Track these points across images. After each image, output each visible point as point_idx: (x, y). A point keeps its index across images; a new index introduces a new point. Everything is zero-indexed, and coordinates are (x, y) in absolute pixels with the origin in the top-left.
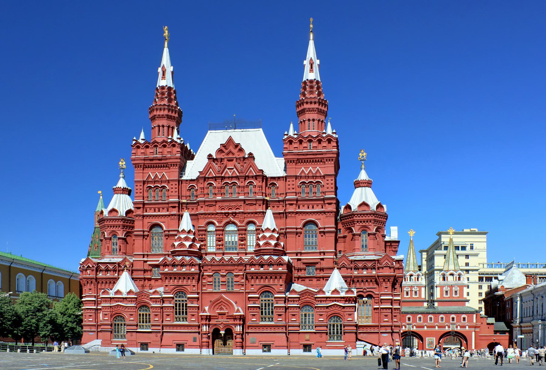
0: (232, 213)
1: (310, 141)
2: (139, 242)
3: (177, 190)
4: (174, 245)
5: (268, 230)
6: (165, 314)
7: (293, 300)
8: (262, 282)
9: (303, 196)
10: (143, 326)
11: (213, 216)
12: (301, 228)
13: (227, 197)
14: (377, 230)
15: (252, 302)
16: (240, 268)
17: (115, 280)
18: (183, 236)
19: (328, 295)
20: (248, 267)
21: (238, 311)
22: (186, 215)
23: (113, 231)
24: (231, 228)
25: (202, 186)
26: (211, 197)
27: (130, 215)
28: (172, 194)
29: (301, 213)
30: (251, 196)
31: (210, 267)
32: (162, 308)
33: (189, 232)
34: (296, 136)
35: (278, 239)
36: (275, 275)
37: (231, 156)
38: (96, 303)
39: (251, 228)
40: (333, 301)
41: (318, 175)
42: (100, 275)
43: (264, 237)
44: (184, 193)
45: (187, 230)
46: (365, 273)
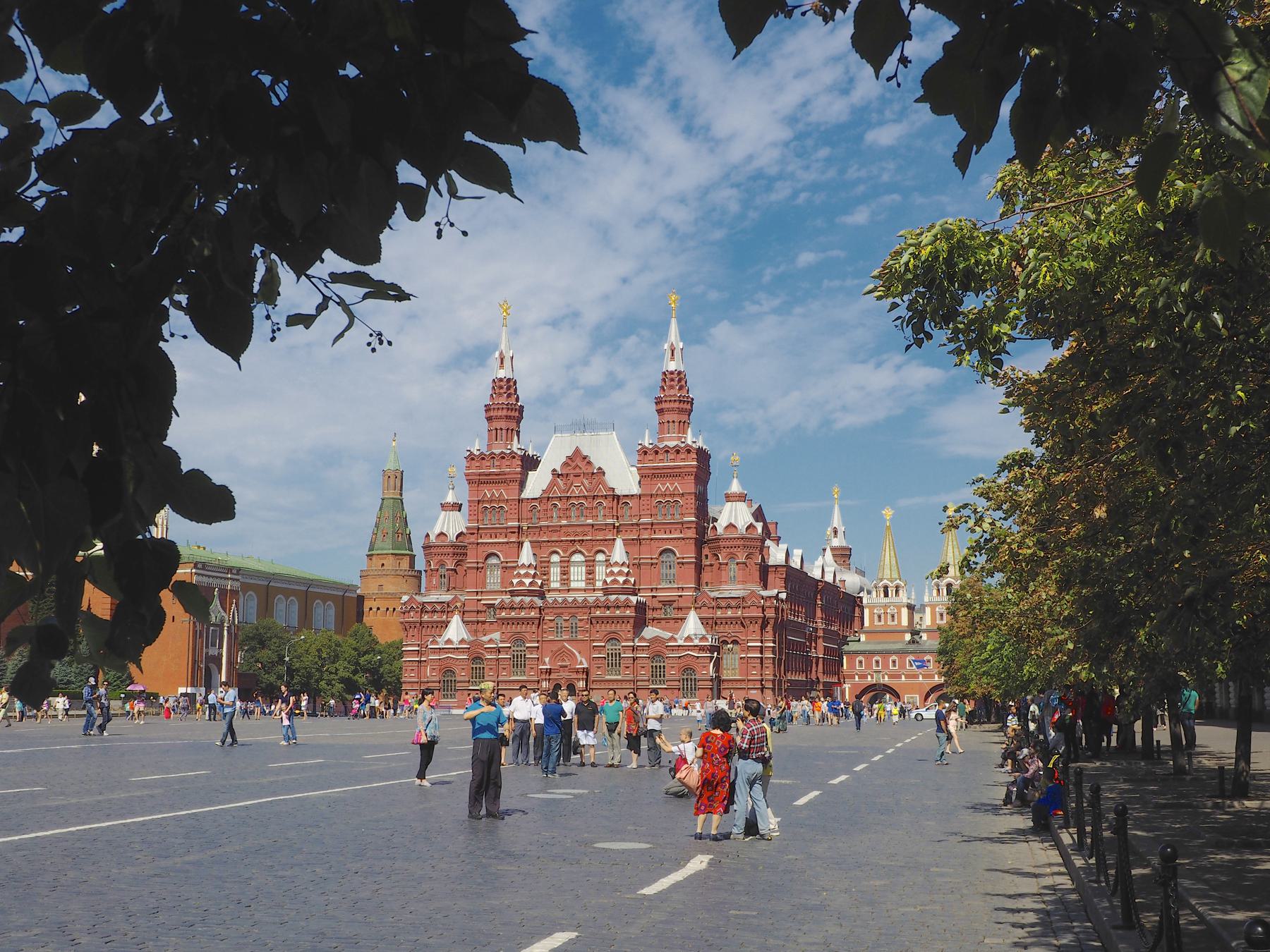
1: (667, 452)
2: (472, 575)
5: (616, 564)
8: (609, 628)
9: (660, 519)
13: (574, 521)
14: (747, 557)
18: (522, 572)
19: (680, 642)
21: (581, 663)
22: (527, 548)
24: (577, 558)
26: (555, 522)
27: (461, 538)
30: (601, 521)
35: (628, 574)
36: (623, 619)
37: (577, 471)
39: (600, 557)
42: (426, 618)
45: (527, 564)
46: (729, 613)
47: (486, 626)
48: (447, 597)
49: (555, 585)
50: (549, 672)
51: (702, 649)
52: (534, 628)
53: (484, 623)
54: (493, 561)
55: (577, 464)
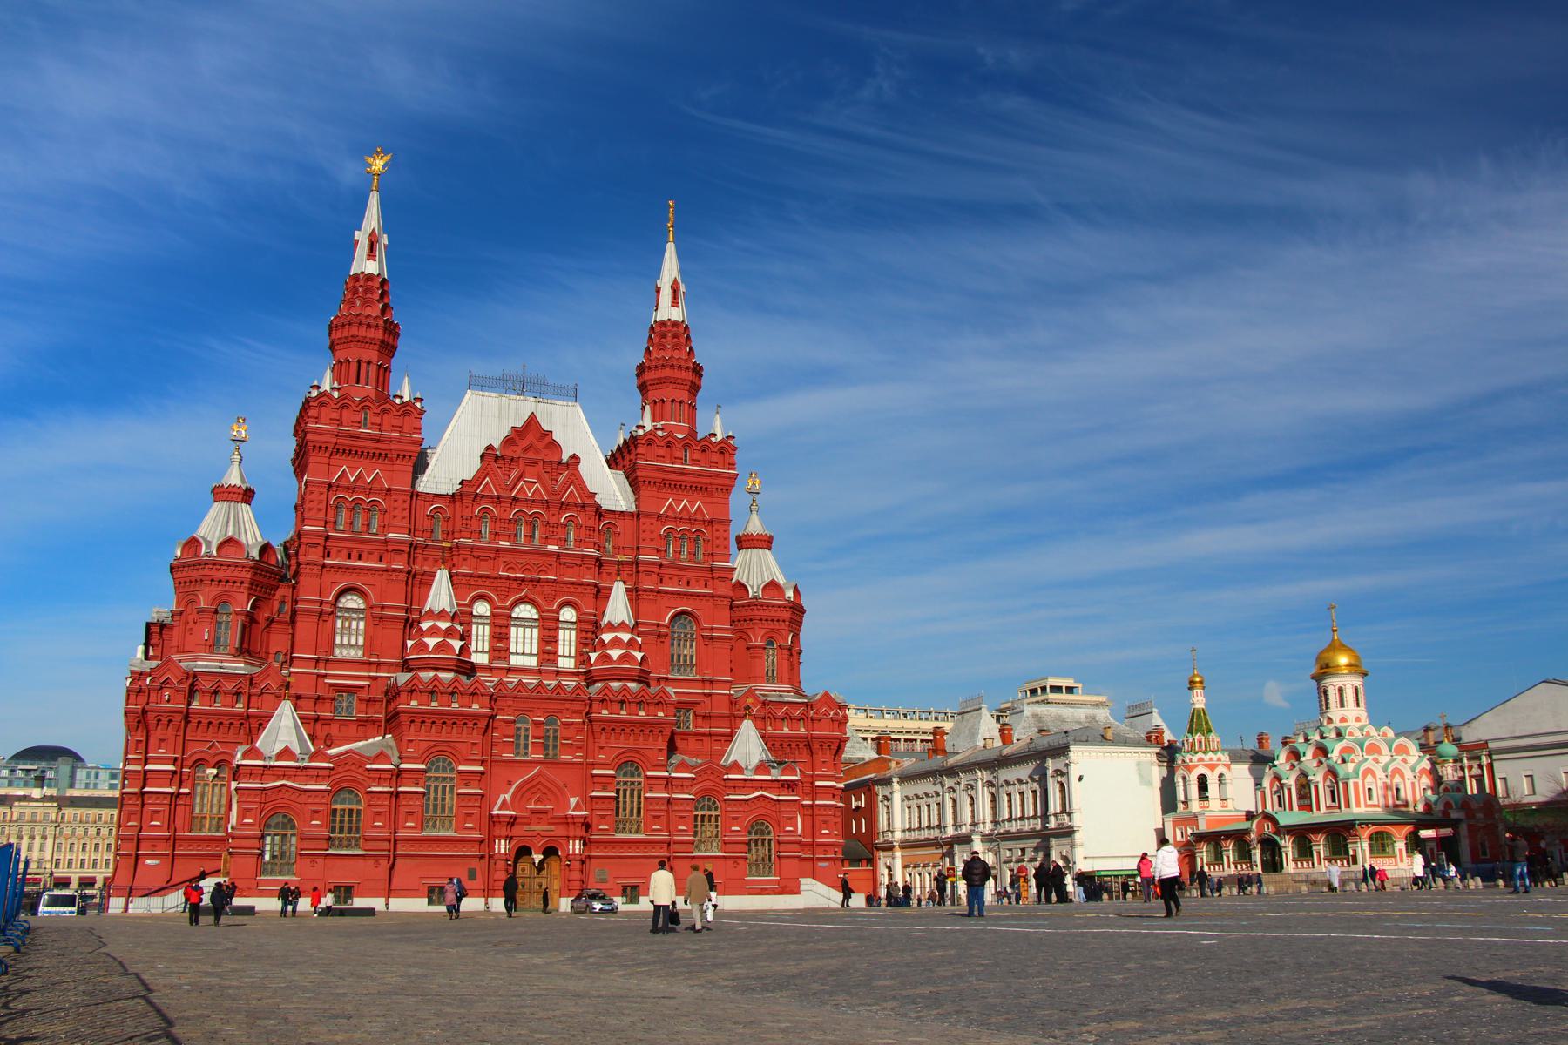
0: (532, 580)
3: (406, 513)
4: (426, 646)
5: (622, 626)
6: (403, 810)
7: (682, 784)
10: (341, 840)
11: (488, 583)
12: (667, 626)
15: (598, 787)
16: (577, 707)
17: (253, 725)
18: (444, 625)
19: (748, 775)
20: (595, 705)
22: (442, 578)
23: (226, 593)
24: (525, 611)
25: (467, 512)
26: (485, 542)
28: (394, 522)
29: (667, 592)
30: (571, 548)
31: (510, 702)
32: (398, 794)
33: (453, 618)
34: (660, 433)
37: (530, 455)
38: (175, 777)
40: (757, 789)
41: (698, 517)
43: (617, 643)
44: (421, 523)
47: (334, 730)
48: (237, 666)
49: (479, 659)
50: (513, 821)
51: (790, 786)
52: (476, 737)
53: (328, 722)
54: (352, 602)
55: (530, 443)
